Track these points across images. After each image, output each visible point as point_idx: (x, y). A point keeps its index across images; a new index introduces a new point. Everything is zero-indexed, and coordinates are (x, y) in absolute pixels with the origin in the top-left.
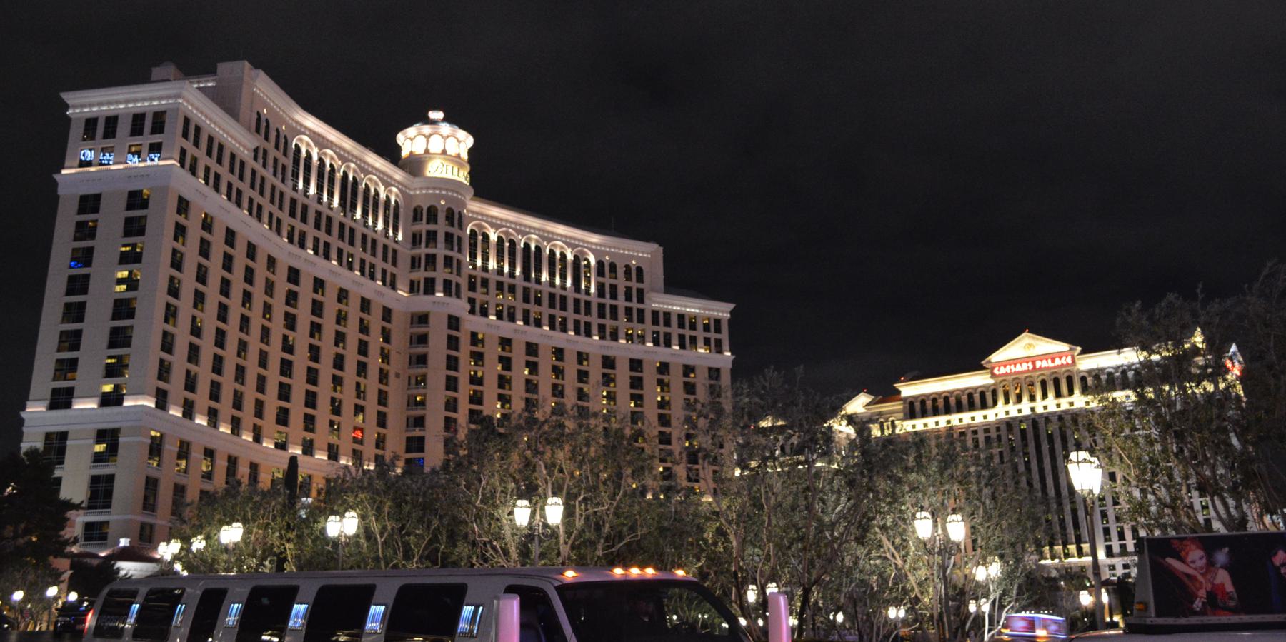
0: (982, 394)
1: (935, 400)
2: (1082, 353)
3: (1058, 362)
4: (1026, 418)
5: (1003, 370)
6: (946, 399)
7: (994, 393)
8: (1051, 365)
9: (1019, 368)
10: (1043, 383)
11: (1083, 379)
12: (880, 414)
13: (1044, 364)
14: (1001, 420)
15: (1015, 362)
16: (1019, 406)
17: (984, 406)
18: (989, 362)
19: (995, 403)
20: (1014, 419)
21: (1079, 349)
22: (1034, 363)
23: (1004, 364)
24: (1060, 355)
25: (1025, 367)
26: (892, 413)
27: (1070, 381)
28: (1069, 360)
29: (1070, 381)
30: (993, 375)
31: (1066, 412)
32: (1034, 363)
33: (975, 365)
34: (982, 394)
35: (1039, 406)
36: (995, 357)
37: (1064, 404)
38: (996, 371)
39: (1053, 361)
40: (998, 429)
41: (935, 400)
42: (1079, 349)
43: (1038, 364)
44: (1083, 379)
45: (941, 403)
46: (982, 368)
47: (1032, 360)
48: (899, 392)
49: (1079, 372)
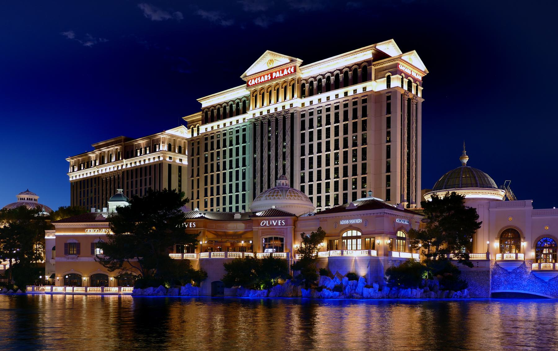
5: (253, 83)
8: (281, 75)
9: (262, 80)
12: (193, 122)
13: (278, 75)
17: (244, 112)
18: (246, 76)
21: (299, 61)
26: (198, 121)
28: (292, 70)
36: (249, 72)
38: (249, 83)
39: (283, 73)
43: (274, 75)
46: (244, 82)
48: (201, 104)
49: (299, 80)
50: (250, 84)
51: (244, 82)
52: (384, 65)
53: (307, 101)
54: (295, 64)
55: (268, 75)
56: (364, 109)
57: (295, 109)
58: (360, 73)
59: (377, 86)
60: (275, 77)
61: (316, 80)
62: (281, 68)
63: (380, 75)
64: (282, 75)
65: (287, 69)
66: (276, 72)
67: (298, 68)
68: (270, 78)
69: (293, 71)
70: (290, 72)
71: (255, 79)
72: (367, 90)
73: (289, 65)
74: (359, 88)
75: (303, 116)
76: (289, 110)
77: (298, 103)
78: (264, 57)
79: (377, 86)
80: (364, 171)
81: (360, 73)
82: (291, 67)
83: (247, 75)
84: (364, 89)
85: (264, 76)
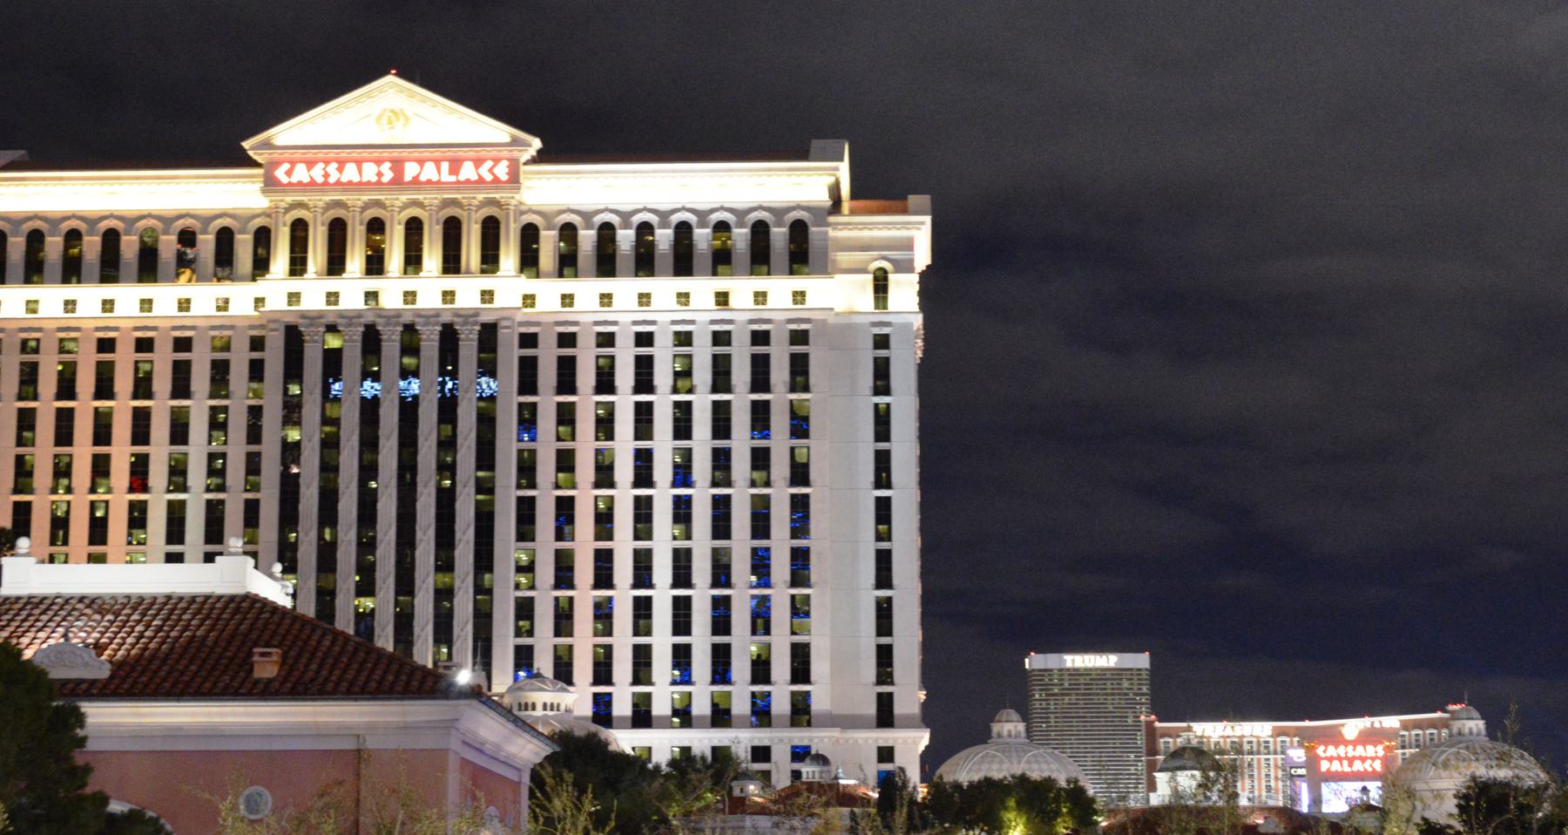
0: (225, 239)
1: (73, 237)
2: (542, 157)
3: (468, 172)
4: (351, 317)
5: (301, 174)
6: (111, 239)
7: (263, 238)
8: (446, 177)
9: (350, 173)
10: (414, 228)
11: (530, 235)
14: (274, 317)
15: (341, 153)
16: (333, 284)
18: (268, 145)
19: (261, 266)
20: (312, 317)
21: (537, 143)
22: (398, 166)
23: (311, 154)
24: (479, 151)
25: (369, 172)
27: (491, 229)
28: (502, 171)
29: (491, 229)
30: (271, 184)
31: (469, 315)
32: (398, 166)
33: (225, 153)
34: (225, 239)
35: (392, 290)
36: (288, 133)
37: (468, 291)
38: (280, 173)
39: (455, 167)
40: (257, 344)
41: (73, 237)
42: (537, 143)
44: (530, 235)
45: (91, 247)
47: (396, 155)
50: (284, 179)
51: (255, 164)
52: (866, 234)
53: (548, 291)
54: (515, 154)
55: (379, 162)
56: (799, 366)
57: (506, 314)
58: (791, 245)
59: (837, 295)
60: (416, 180)
61: (589, 226)
62: (453, 154)
63: (843, 258)
64: (453, 178)
65: (478, 162)
66: (421, 162)
67: (523, 168)
68: (388, 176)
69: (504, 177)
70: (488, 177)
71: (310, 164)
72: (810, 303)
73: (505, 153)
74: (779, 288)
75: (529, 340)
76: (476, 313)
77: (509, 289)
78: (369, 95)
79: (837, 295)
80: (800, 574)
81: (791, 245)
82: (497, 161)
83: (278, 142)
84: (799, 296)
85: (359, 163)
